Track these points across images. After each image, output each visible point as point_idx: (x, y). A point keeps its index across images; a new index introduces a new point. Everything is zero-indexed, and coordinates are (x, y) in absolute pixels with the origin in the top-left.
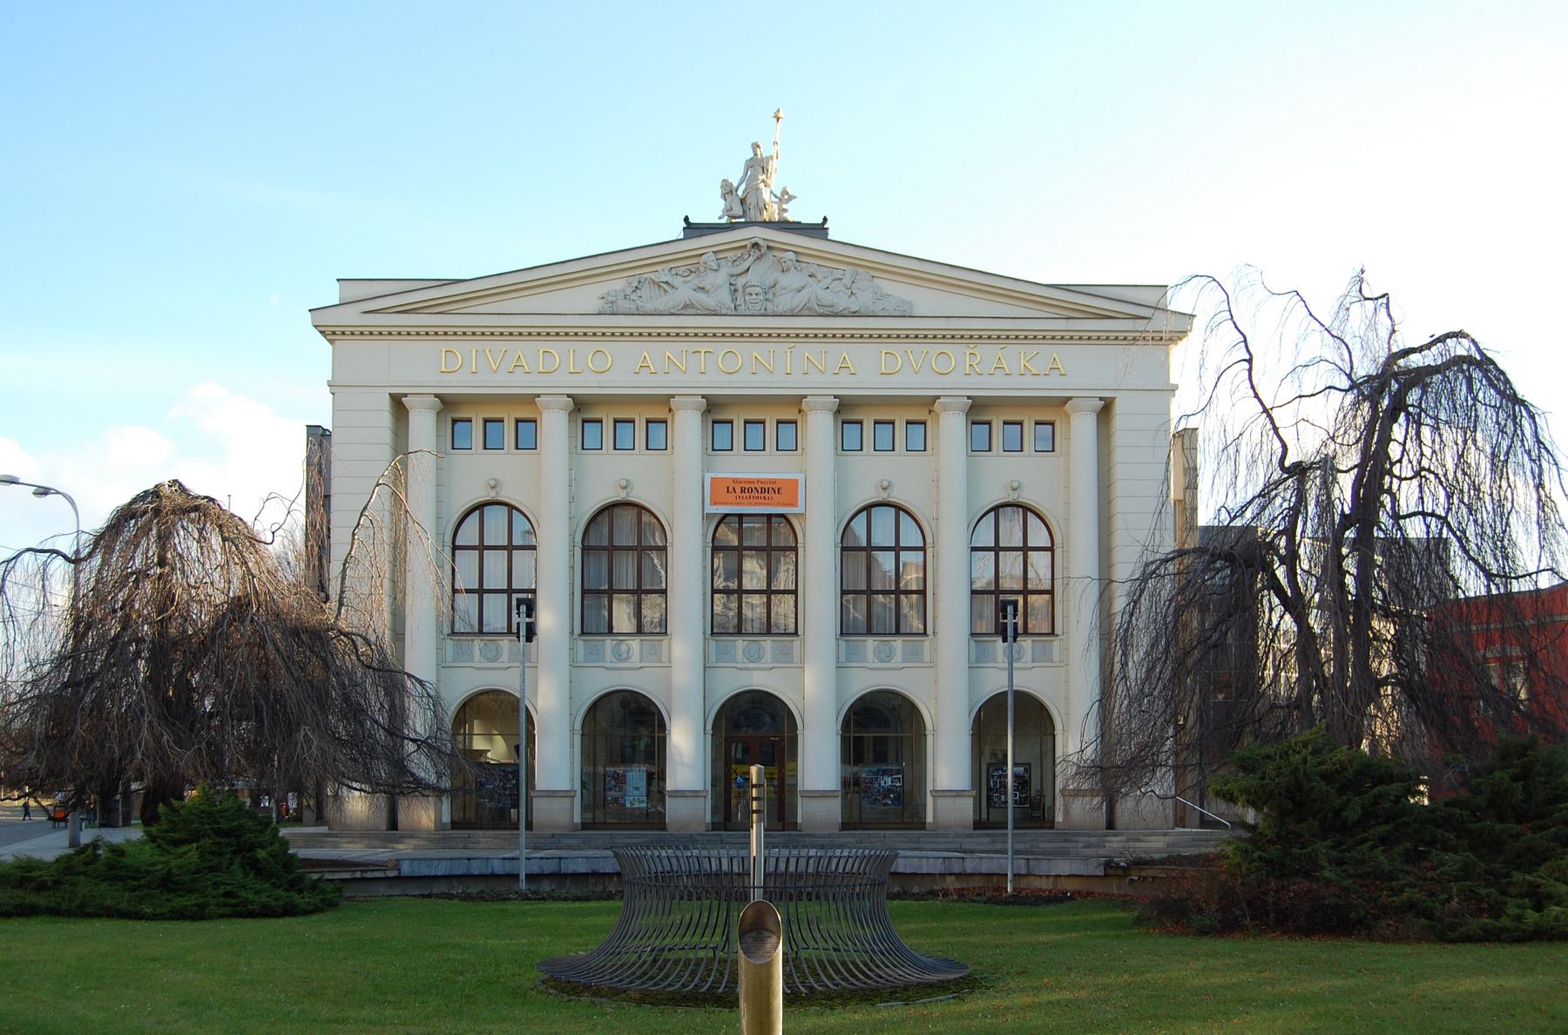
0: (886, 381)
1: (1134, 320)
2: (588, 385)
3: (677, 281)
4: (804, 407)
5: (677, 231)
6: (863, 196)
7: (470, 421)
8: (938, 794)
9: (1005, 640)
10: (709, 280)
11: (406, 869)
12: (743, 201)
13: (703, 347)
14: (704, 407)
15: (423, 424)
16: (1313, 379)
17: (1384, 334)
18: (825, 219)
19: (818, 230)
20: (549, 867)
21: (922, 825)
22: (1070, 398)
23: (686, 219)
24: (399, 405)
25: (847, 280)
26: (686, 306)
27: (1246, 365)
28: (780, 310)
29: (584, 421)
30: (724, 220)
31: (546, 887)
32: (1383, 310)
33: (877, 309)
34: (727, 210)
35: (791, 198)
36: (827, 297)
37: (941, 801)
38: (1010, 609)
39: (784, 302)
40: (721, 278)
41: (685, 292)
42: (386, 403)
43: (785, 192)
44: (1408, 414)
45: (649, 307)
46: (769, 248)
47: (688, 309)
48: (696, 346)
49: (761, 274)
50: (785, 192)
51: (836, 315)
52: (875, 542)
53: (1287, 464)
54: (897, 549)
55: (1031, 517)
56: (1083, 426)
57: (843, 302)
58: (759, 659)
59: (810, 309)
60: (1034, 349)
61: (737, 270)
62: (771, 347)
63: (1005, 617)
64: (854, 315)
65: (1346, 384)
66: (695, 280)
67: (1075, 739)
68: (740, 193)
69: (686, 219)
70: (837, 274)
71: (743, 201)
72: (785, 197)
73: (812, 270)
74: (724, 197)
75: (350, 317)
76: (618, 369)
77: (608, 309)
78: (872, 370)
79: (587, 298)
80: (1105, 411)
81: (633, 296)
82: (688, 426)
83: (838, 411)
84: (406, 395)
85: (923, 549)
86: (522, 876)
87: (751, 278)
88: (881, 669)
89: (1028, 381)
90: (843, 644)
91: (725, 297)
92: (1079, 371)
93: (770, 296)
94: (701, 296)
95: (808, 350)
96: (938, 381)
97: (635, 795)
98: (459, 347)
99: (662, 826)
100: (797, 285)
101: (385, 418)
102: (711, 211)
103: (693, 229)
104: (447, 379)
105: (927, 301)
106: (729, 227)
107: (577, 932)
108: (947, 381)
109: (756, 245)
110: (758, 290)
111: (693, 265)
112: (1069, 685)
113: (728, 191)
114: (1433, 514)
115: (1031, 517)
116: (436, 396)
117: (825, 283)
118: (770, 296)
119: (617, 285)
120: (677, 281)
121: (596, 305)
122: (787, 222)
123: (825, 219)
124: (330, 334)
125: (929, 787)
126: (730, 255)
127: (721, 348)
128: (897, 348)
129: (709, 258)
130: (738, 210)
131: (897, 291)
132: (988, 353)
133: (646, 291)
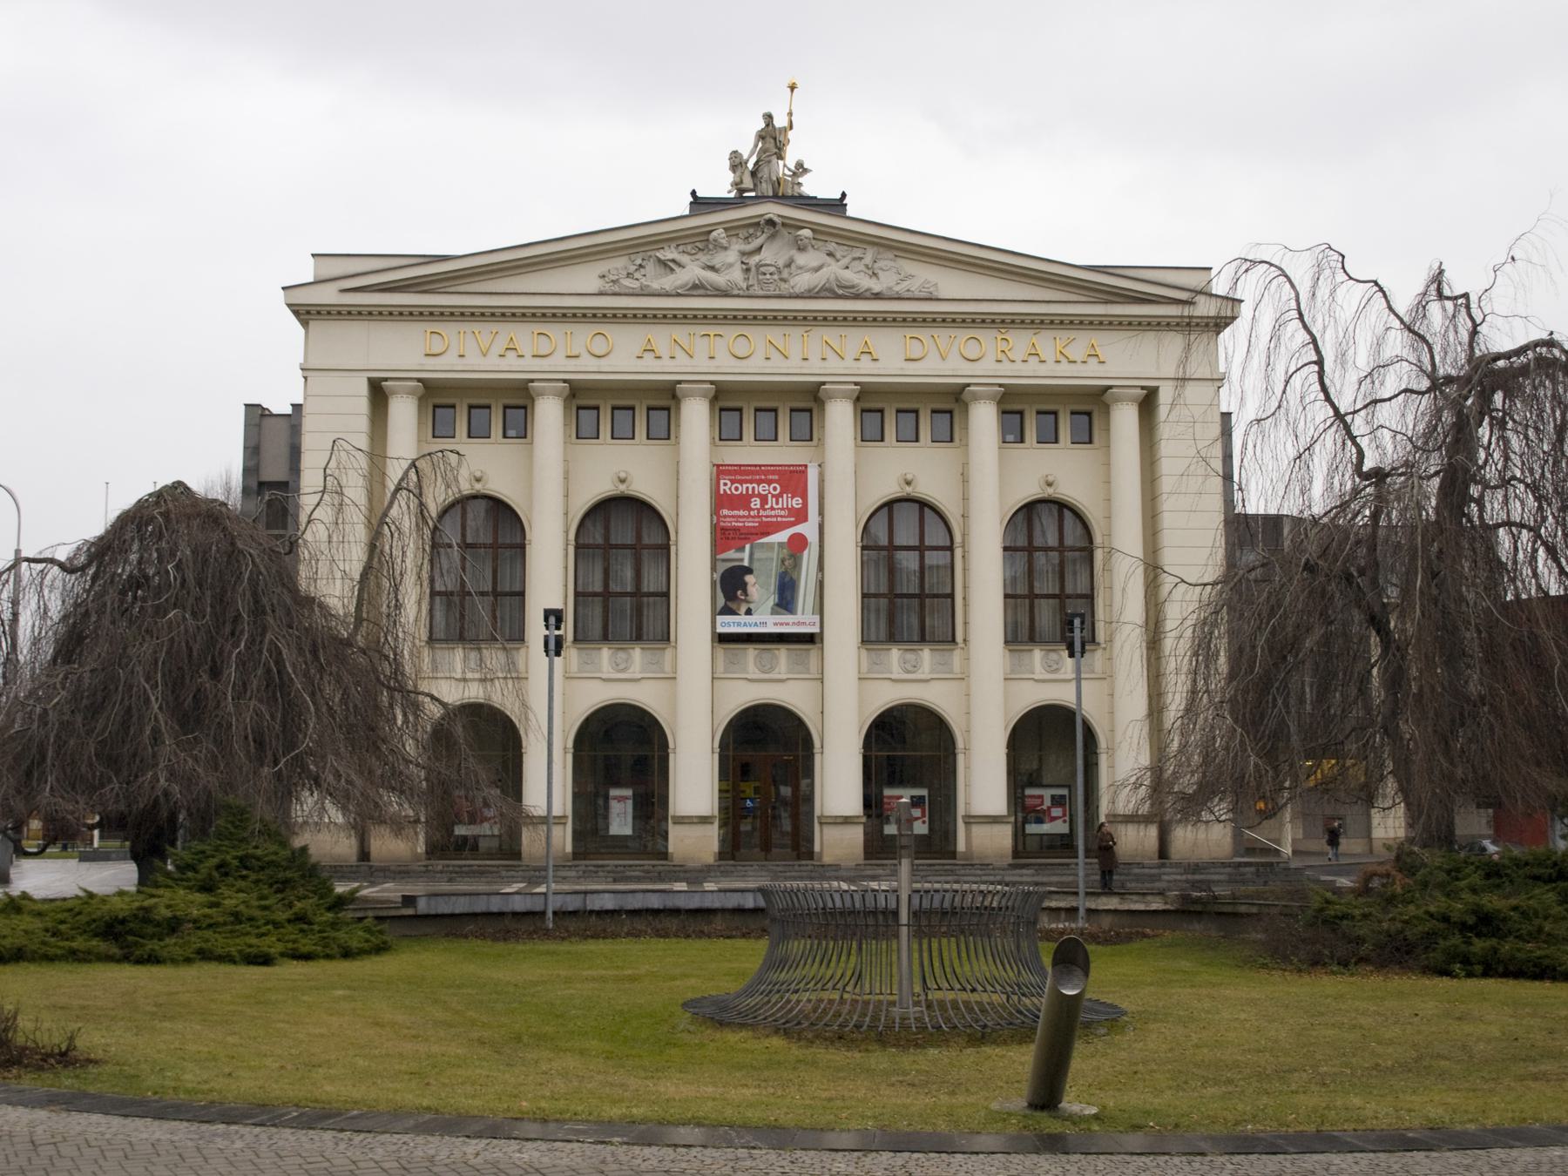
1: (1184, 310)
2: (588, 368)
3: (684, 259)
4: (821, 394)
6: (871, 165)
7: (453, 407)
8: (971, 820)
9: (1071, 655)
10: (719, 259)
11: (423, 907)
12: (754, 174)
13: (712, 330)
14: (712, 394)
15: (403, 412)
16: (1391, 383)
17: (1464, 336)
18: (844, 195)
19: (837, 206)
20: (573, 903)
21: (953, 854)
22: (1111, 387)
23: (693, 193)
24: (378, 393)
25: (868, 259)
26: (695, 286)
27: (1316, 368)
28: (797, 290)
29: (579, 408)
30: (732, 195)
31: (573, 925)
32: (1463, 310)
33: (900, 288)
34: (736, 184)
35: (806, 171)
36: (849, 276)
37: (977, 830)
38: (1077, 622)
39: (803, 281)
40: (732, 256)
41: (692, 271)
42: (363, 388)
43: (800, 165)
44: (1492, 418)
45: (655, 286)
46: (784, 225)
47: (697, 288)
49: (773, 254)
50: (800, 165)
51: (858, 297)
52: (898, 541)
53: (1365, 469)
54: (921, 549)
55: (1067, 513)
56: (1125, 419)
57: (865, 283)
58: (771, 670)
59: (831, 290)
60: (1072, 334)
62: (788, 330)
63: (1072, 631)
64: (877, 296)
65: (1425, 384)
66: (704, 258)
67: (1125, 761)
68: (750, 165)
69: (693, 193)
70: (858, 253)
72: (801, 169)
73: (832, 247)
74: (734, 168)
75: (328, 296)
76: (624, 356)
77: (608, 287)
78: (895, 358)
80: (1148, 403)
81: (637, 275)
82: (696, 416)
83: (858, 399)
84: (386, 379)
85: (951, 549)
86: (550, 915)
87: (767, 256)
88: (911, 678)
89: (1065, 369)
90: (864, 653)
91: (736, 275)
92: (1121, 360)
96: (968, 368)
97: (621, 822)
98: (451, 331)
100: (815, 264)
101: (362, 404)
102: (720, 185)
104: (431, 363)
106: (739, 201)
107: (729, 965)
109: (771, 223)
110: (772, 269)
111: (700, 241)
112: (1130, 703)
113: (736, 163)
114: (1522, 526)
115: (1067, 513)
116: (419, 380)
117: (845, 262)
118: (785, 275)
119: (618, 264)
120: (684, 259)
121: (594, 285)
122: (801, 197)
123: (844, 195)
124: (304, 314)
125: (961, 811)
126: (743, 233)
128: (924, 334)
129: (719, 234)
131: (923, 276)
132: (1020, 341)
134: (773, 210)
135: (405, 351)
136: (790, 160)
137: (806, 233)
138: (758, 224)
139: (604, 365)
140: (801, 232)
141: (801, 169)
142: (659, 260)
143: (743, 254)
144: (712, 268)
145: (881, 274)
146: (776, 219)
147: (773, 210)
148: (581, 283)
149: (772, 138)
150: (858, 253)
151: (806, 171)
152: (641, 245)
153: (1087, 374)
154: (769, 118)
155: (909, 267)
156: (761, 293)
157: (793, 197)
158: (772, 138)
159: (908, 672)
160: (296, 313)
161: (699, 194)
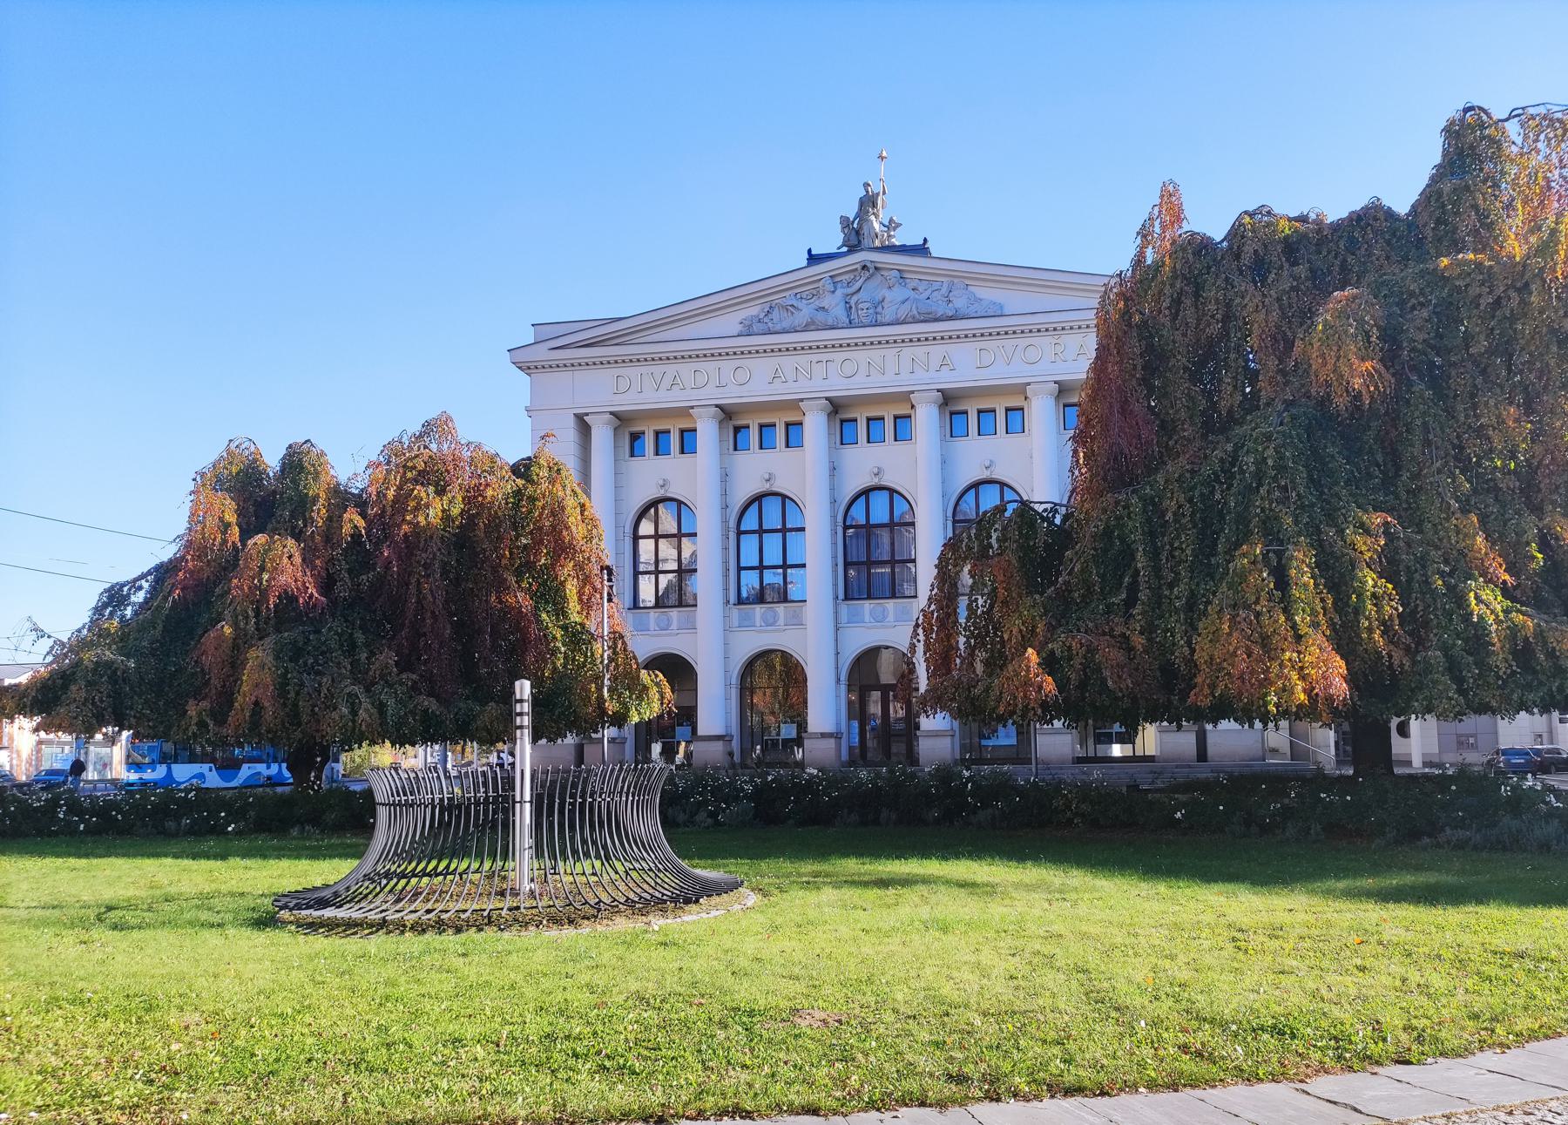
15: (602, 436)
19: (921, 250)
35: (899, 225)
43: (891, 220)
49: (873, 290)
50: (891, 220)
51: (936, 320)
57: (941, 310)
61: (851, 290)
72: (891, 225)
75: (542, 354)
76: (755, 382)
79: (730, 323)
93: (879, 309)
94: (820, 316)
103: (813, 259)
121: (738, 328)
124: (526, 368)
133: (775, 314)
135: (604, 391)
136: (884, 216)
149: (868, 202)
151: (899, 225)
154: (866, 185)
158: (868, 202)
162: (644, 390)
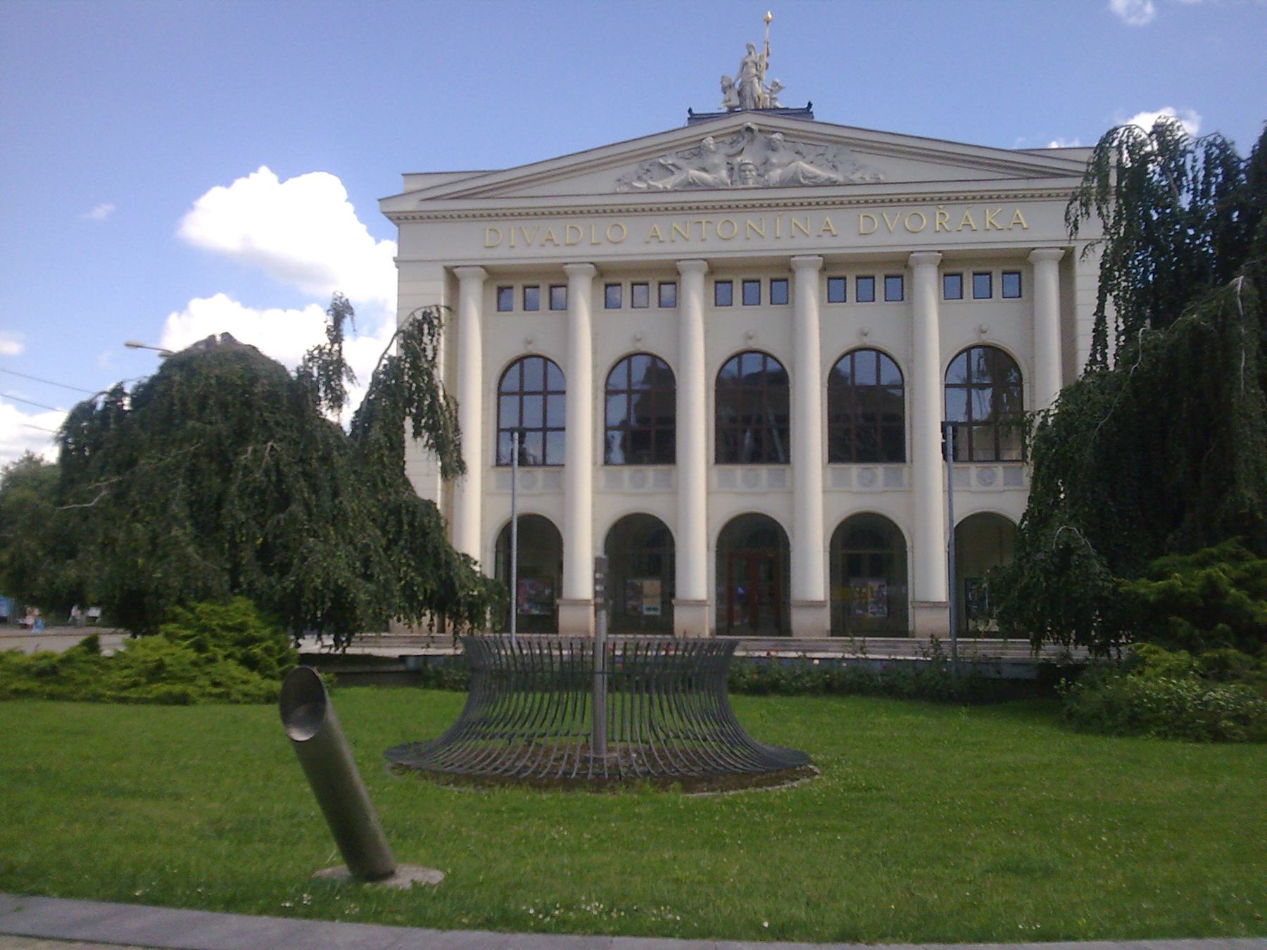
0: (863, 241)
2: (608, 253)
3: (681, 163)
5: (683, 120)
13: (704, 219)
18: (810, 105)
19: (806, 113)
23: (690, 111)
24: (453, 280)
25: (830, 156)
35: (781, 88)
40: (718, 159)
42: (441, 273)
48: (698, 218)
57: (824, 174)
61: (732, 151)
68: (737, 86)
69: (690, 111)
70: (821, 151)
71: (740, 94)
72: (776, 87)
74: (724, 90)
76: (634, 242)
78: (854, 234)
91: (724, 174)
95: (796, 218)
96: (911, 239)
99: (670, 630)
103: (694, 118)
104: (489, 253)
105: (898, 171)
108: (920, 239)
109: (749, 129)
111: (698, 151)
116: (482, 267)
120: (681, 163)
123: (810, 105)
127: (719, 220)
129: (709, 141)
130: (735, 101)
134: (751, 120)
135: (476, 245)
137: (777, 136)
138: (739, 132)
139: (620, 249)
140: (774, 136)
141: (776, 87)
142: (662, 166)
143: (729, 156)
144: (704, 170)
145: (839, 166)
146: (754, 127)
147: (751, 120)
148: (599, 186)
150: (821, 151)
151: (781, 88)
152: (647, 155)
153: (1012, 239)
155: (862, 158)
156: (741, 186)
157: (770, 109)
159: (865, 485)
160: (390, 218)
161: (694, 112)
162: (522, 246)
